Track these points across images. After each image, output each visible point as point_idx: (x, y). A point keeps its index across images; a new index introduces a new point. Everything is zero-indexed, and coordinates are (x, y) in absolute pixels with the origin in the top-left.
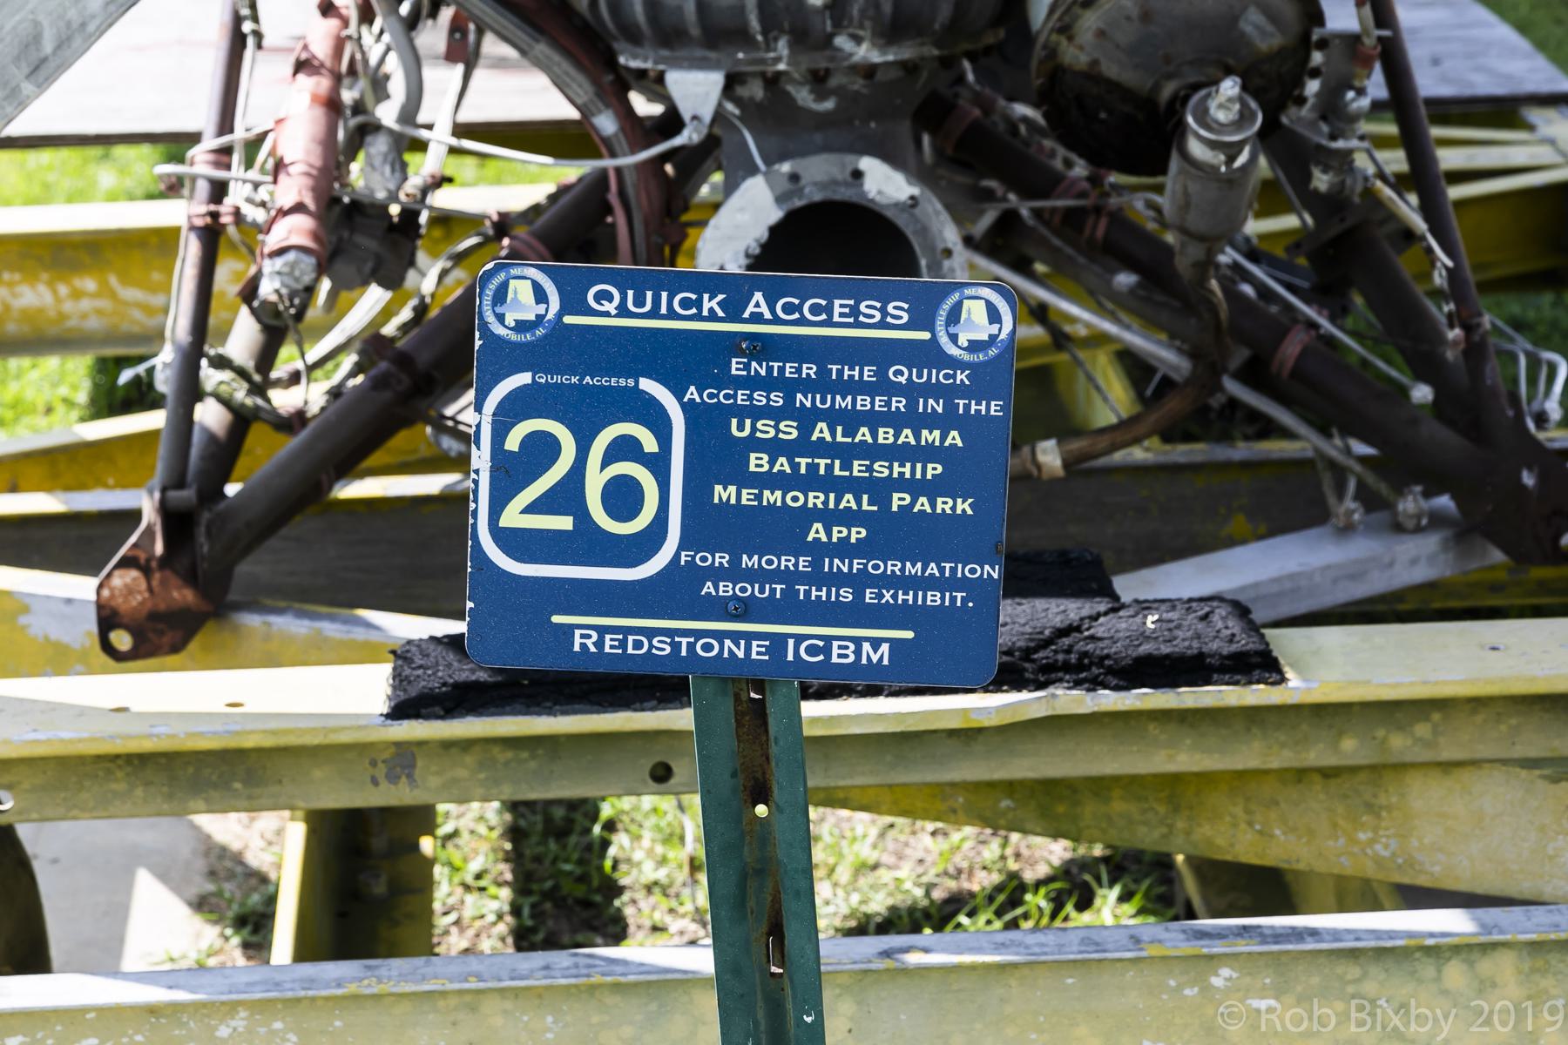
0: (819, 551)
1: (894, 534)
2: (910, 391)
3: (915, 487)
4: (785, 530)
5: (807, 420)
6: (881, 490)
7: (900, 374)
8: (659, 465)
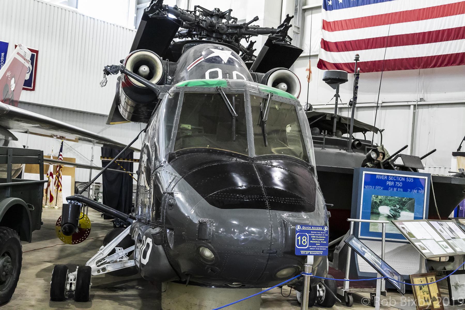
0: (317, 246)
1: (322, 244)
2: (322, 234)
3: (323, 241)
4: (314, 244)
5: (316, 236)
6: (320, 241)
7: (321, 233)
8: (307, 240)
